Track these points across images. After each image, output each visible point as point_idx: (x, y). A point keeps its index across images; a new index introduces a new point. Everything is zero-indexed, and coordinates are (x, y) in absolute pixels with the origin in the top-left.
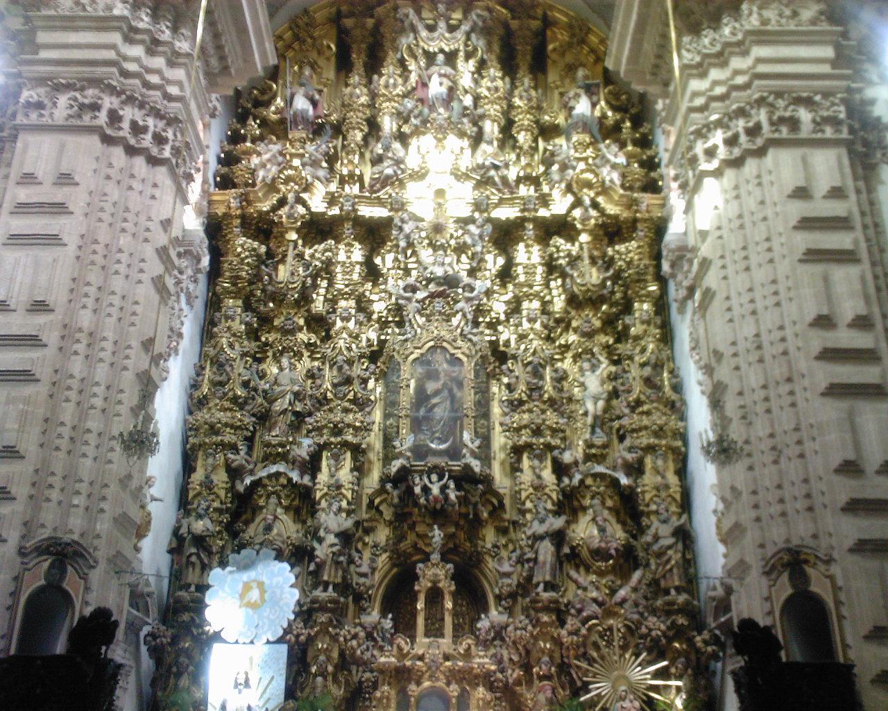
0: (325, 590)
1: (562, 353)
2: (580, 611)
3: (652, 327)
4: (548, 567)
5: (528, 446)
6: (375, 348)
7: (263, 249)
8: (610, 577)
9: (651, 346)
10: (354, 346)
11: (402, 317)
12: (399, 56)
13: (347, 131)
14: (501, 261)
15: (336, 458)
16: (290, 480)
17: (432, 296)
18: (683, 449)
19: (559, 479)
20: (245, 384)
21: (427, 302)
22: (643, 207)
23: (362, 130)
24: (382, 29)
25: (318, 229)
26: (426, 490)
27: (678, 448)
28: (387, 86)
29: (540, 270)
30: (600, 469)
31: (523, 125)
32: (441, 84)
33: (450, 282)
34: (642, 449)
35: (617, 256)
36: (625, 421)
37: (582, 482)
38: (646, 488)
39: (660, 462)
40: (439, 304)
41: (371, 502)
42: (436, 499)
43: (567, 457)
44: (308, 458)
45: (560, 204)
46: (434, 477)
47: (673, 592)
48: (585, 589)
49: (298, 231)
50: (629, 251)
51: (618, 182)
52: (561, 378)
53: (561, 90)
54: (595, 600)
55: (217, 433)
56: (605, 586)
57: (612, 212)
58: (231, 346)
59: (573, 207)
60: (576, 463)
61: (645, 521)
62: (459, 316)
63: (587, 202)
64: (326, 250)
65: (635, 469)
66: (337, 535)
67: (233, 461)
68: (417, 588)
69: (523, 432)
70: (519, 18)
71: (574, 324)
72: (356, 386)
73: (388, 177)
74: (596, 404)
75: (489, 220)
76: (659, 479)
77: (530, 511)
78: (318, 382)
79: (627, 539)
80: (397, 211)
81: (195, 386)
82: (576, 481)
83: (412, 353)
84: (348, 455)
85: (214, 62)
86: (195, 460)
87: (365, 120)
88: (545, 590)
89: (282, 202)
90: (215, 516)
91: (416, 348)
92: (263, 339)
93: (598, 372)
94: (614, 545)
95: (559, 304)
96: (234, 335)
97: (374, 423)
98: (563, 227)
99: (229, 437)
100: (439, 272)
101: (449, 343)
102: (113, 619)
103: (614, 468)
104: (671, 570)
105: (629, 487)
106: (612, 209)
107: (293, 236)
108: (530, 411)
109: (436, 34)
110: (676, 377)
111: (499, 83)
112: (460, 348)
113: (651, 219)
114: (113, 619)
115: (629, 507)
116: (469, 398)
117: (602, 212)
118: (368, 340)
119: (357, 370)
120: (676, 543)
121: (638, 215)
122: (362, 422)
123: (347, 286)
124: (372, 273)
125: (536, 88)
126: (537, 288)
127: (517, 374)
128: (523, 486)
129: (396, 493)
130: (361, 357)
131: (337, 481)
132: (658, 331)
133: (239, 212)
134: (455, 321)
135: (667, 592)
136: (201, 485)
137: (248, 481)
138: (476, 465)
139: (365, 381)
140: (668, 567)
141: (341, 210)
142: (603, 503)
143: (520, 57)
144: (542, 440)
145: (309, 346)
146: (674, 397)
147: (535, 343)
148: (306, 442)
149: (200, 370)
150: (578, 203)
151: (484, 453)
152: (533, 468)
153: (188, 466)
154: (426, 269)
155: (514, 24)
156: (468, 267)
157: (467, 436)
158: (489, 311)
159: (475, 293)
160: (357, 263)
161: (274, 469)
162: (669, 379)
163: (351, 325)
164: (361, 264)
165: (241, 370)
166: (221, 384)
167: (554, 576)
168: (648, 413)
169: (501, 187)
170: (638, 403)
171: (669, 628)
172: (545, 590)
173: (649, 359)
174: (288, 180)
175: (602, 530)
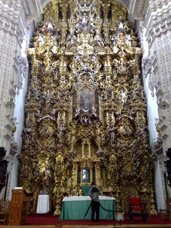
0: (60, 144)
1: (116, 89)
2: (121, 149)
3: (138, 81)
4: (113, 138)
5: (108, 110)
6: (70, 88)
7: (42, 63)
8: (128, 141)
9: (138, 86)
10: (65, 87)
11: (76, 80)
12: (74, 14)
13: (62, 33)
14: (100, 66)
15: (62, 113)
16: (51, 119)
17: (84, 74)
18: (146, 111)
19: (115, 118)
20: (39, 97)
21: (83, 76)
22: (137, 51)
23: (65, 33)
24: (70, 7)
25: (55, 57)
26: (83, 121)
27: (145, 110)
28: (71, 21)
29: (110, 68)
30: (125, 116)
31: (106, 31)
32: (86, 20)
33: (88, 71)
34: (136, 111)
35: (130, 63)
36: (132, 104)
37: (121, 119)
38: (137, 120)
39: (140, 114)
40: (85, 77)
41: (70, 124)
42: (86, 124)
43: (117, 113)
44: (55, 114)
45: (116, 50)
46: (85, 118)
47: (144, 144)
48: (122, 144)
50: (133, 62)
51: (130, 44)
52: (115, 94)
53: (115, 22)
54: (125, 146)
55: (32, 108)
56: (127, 143)
57: (129, 52)
58: (35, 87)
59: (119, 52)
60: (120, 114)
61: (137, 128)
62: (90, 79)
63: (123, 50)
64: (57, 63)
65: (134, 116)
66: (62, 131)
67: (37, 115)
68: (82, 144)
69: (107, 107)
70: (104, 4)
71: (119, 81)
72: (66, 97)
73: (72, 44)
74: (124, 100)
75: (98, 55)
76: (140, 118)
77: (109, 126)
78: (57, 96)
79: (132, 132)
80: (75, 53)
81: (27, 97)
82: (119, 119)
83: (79, 88)
84: (64, 113)
85: (27, 11)
86: (27, 115)
87: (66, 31)
88: (113, 144)
89: (46, 51)
90: (32, 127)
91: (80, 87)
92: (43, 86)
93: (125, 93)
94: (129, 134)
95: (115, 76)
96: (36, 85)
97: (70, 106)
98: (115, 56)
99: (35, 109)
100: (85, 68)
101: (88, 85)
102: (5, 150)
103: (129, 116)
104: (144, 139)
105: (133, 120)
108: (108, 102)
109: (84, 7)
110: (144, 93)
111: (100, 20)
112: (91, 87)
113: (139, 54)
114: (5, 150)
115: (132, 123)
116: (93, 99)
117: (126, 53)
118: (68, 86)
119: (66, 93)
120: (145, 133)
121: (135, 53)
122: (67, 105)
123: (63, 72)
124: (69, 69)
125: (109, 22)
126: (110, 72)
127: (105, 93)
128: (107, 120)
129: (76, 122)
130: (67, 90)
131: (62, 119)
132: (140, 82)
133: (35, 54)
134: (90, 81)
135: (142, 144)
136: (29, 120)
137: (40, 119)
138: (96, 115)
139: (68, 96)
140: (143, 138)
141: (61, 53)
143: (105, 14)
144: (111, 109)
145: (54, 87)
146: (144, 98)
147: (110, 86)
148: (54, 110)
149: (27, 93)
150: (120, 50)
151: (97, 112)
152: (109, 116)
153: (26, 116)
154: (82, 68)
155: (103, 5)
156: (92, 67)
157: (93, 108)
158: (98, 78)
159: (95, 73)
160: (65, 67)
161: (46, 117)
162: (143, 94)
163: (64, 82)
164: (66, 67)
165: (38, 93)
166: (33, 96)
167: (115, 140)
168: (137, 102)
169: (101, 46)
170: (135, 100)
171: (143, 153)
172: (113, 144)
173: (138, 89)
175: (126, 130)
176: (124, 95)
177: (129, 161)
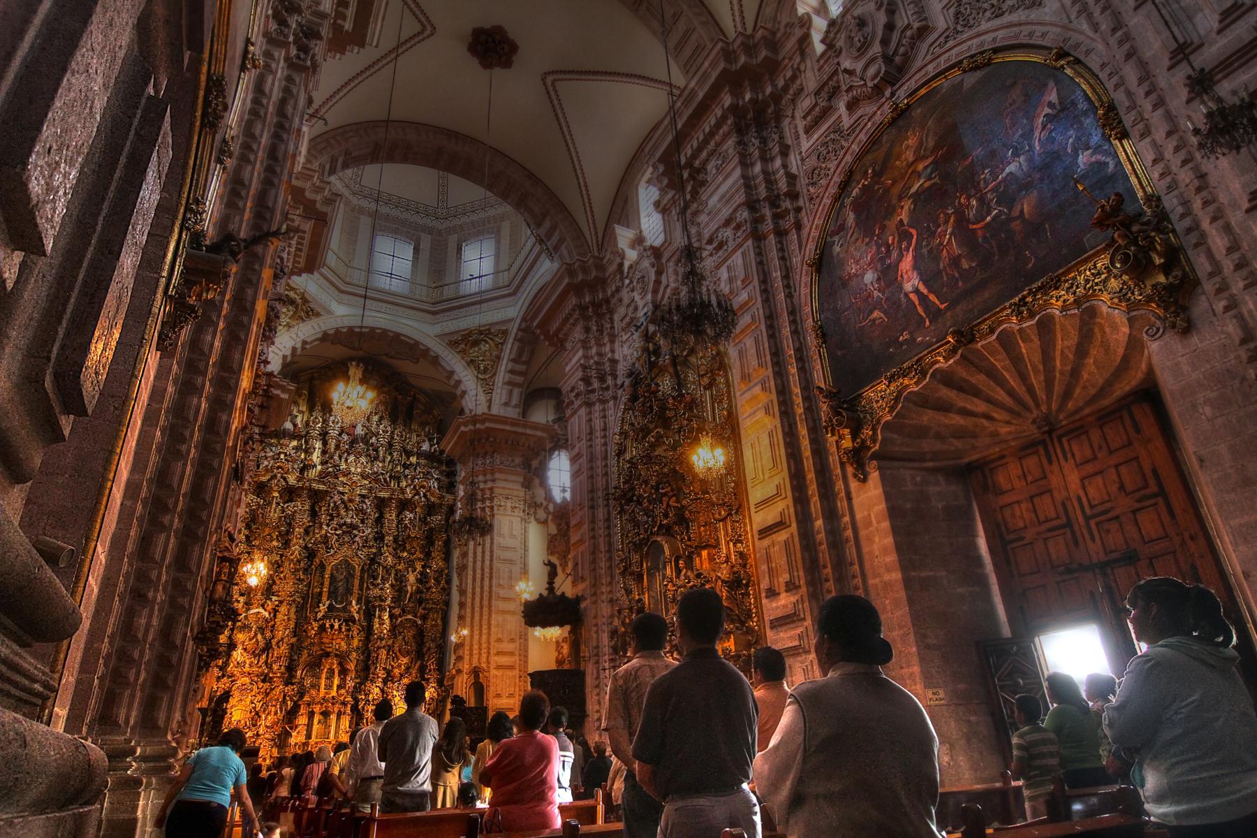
33: (353, 526)
50: (437, 519)
65: (424, 618)
107: (276, 494)
117: (428, 500)
176: (412, 578)
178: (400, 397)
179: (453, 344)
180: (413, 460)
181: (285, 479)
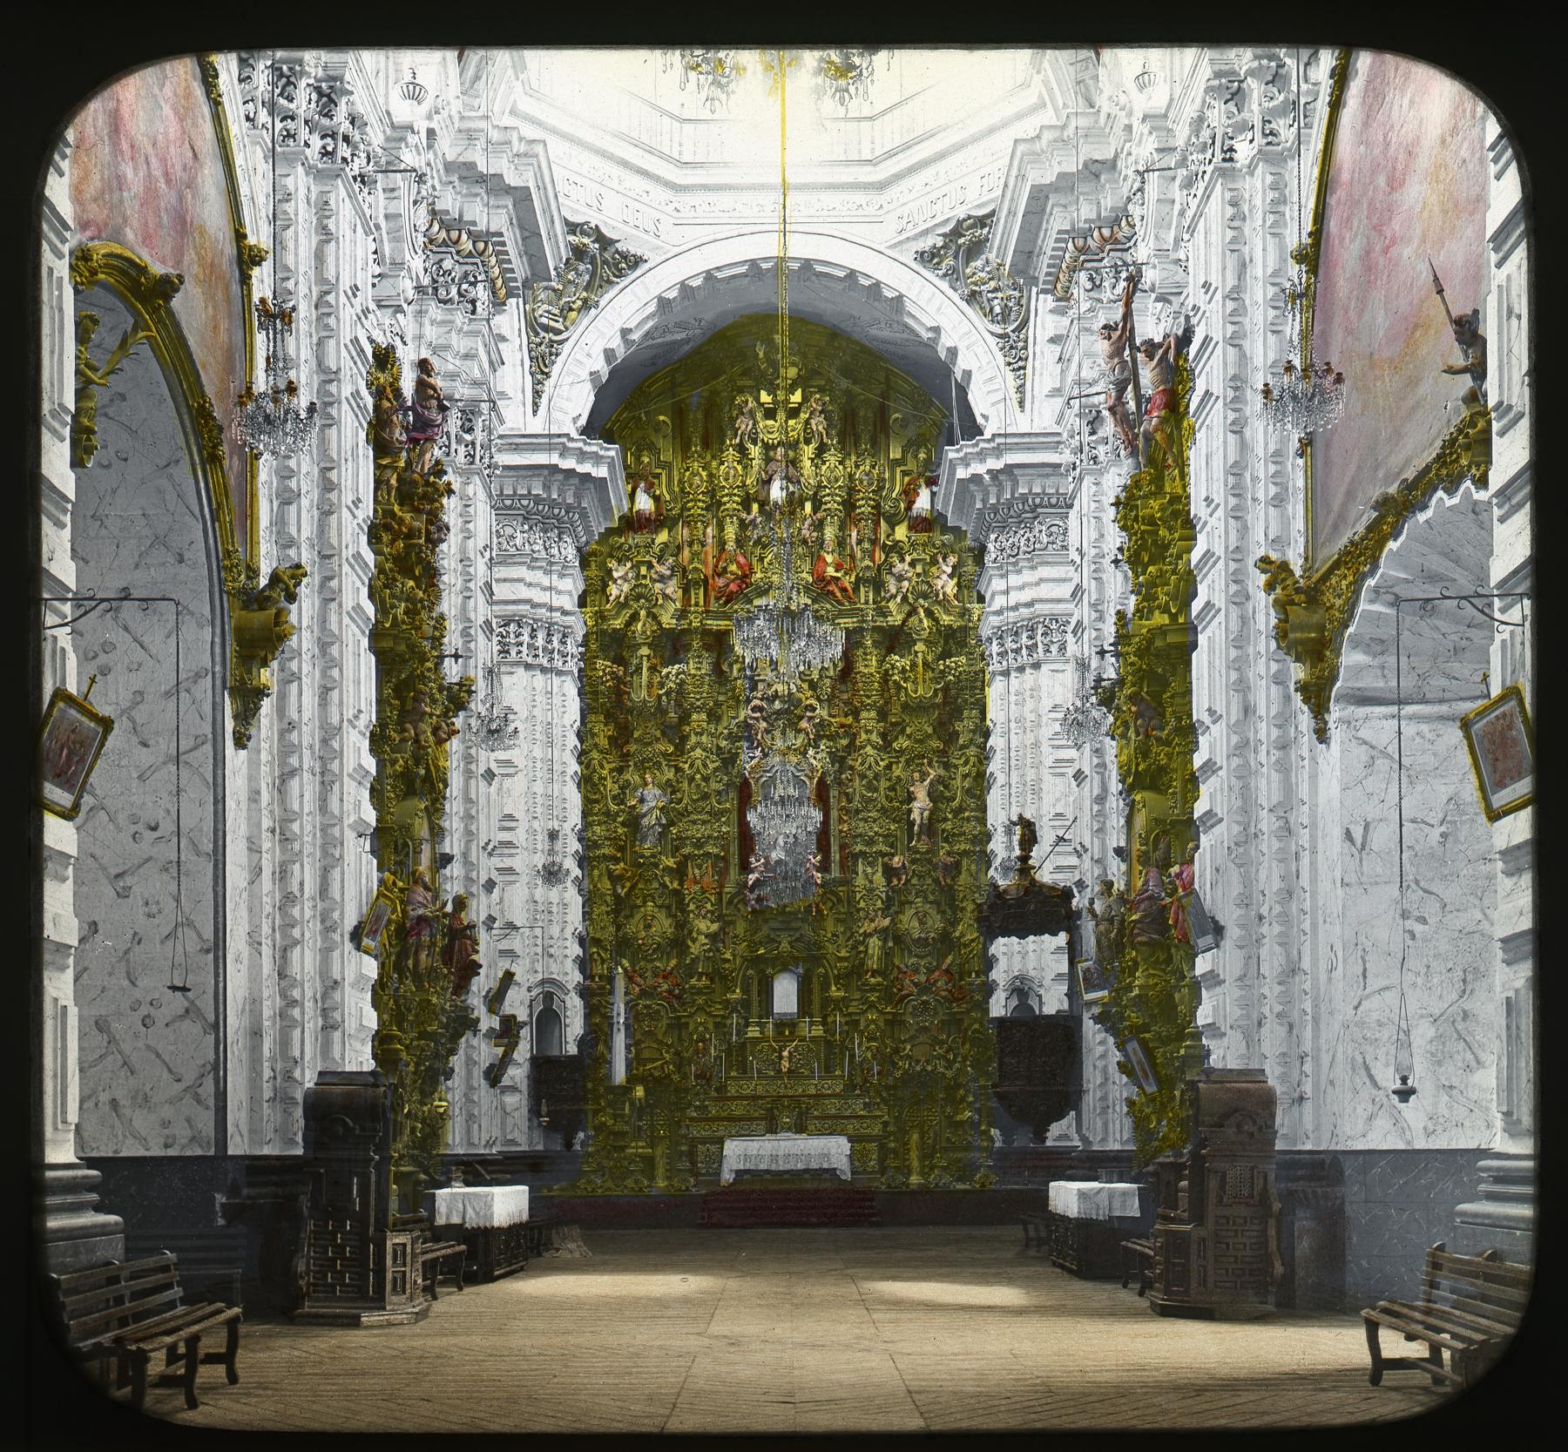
5: (862, 853)
19: (889, 882)
37: (908, 881)
43: (897, 861)
49: (650, 646)
64: (678, 674)
106: (946, 619)
142: (925, 898)
170: (960, 810)
174: (638, 597)
177: (926, 1029)
178: (857, 389)
179: (929, 258)
180: (901, 532)
181: (655, 617)
